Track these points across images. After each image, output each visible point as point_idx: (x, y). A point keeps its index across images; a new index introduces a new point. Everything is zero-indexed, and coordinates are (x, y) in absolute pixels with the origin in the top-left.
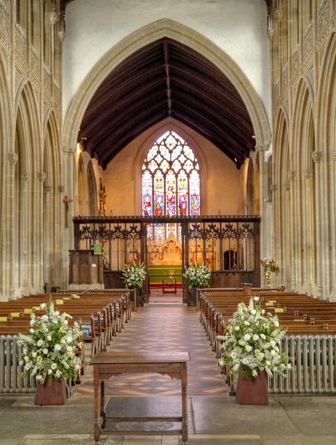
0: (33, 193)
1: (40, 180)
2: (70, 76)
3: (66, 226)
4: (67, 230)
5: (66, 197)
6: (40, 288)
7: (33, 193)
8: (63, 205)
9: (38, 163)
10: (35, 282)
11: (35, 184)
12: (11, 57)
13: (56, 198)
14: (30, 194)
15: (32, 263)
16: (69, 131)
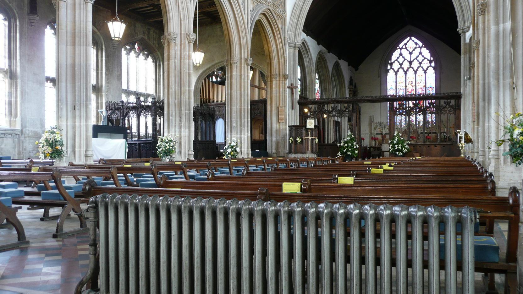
0: (241, 76)
1: (247, 64)
3: (293, 108)
5: (292, 84)
7: (241, 76)
11: (243, 68)
14: (238, 77)
15: (241, 134)
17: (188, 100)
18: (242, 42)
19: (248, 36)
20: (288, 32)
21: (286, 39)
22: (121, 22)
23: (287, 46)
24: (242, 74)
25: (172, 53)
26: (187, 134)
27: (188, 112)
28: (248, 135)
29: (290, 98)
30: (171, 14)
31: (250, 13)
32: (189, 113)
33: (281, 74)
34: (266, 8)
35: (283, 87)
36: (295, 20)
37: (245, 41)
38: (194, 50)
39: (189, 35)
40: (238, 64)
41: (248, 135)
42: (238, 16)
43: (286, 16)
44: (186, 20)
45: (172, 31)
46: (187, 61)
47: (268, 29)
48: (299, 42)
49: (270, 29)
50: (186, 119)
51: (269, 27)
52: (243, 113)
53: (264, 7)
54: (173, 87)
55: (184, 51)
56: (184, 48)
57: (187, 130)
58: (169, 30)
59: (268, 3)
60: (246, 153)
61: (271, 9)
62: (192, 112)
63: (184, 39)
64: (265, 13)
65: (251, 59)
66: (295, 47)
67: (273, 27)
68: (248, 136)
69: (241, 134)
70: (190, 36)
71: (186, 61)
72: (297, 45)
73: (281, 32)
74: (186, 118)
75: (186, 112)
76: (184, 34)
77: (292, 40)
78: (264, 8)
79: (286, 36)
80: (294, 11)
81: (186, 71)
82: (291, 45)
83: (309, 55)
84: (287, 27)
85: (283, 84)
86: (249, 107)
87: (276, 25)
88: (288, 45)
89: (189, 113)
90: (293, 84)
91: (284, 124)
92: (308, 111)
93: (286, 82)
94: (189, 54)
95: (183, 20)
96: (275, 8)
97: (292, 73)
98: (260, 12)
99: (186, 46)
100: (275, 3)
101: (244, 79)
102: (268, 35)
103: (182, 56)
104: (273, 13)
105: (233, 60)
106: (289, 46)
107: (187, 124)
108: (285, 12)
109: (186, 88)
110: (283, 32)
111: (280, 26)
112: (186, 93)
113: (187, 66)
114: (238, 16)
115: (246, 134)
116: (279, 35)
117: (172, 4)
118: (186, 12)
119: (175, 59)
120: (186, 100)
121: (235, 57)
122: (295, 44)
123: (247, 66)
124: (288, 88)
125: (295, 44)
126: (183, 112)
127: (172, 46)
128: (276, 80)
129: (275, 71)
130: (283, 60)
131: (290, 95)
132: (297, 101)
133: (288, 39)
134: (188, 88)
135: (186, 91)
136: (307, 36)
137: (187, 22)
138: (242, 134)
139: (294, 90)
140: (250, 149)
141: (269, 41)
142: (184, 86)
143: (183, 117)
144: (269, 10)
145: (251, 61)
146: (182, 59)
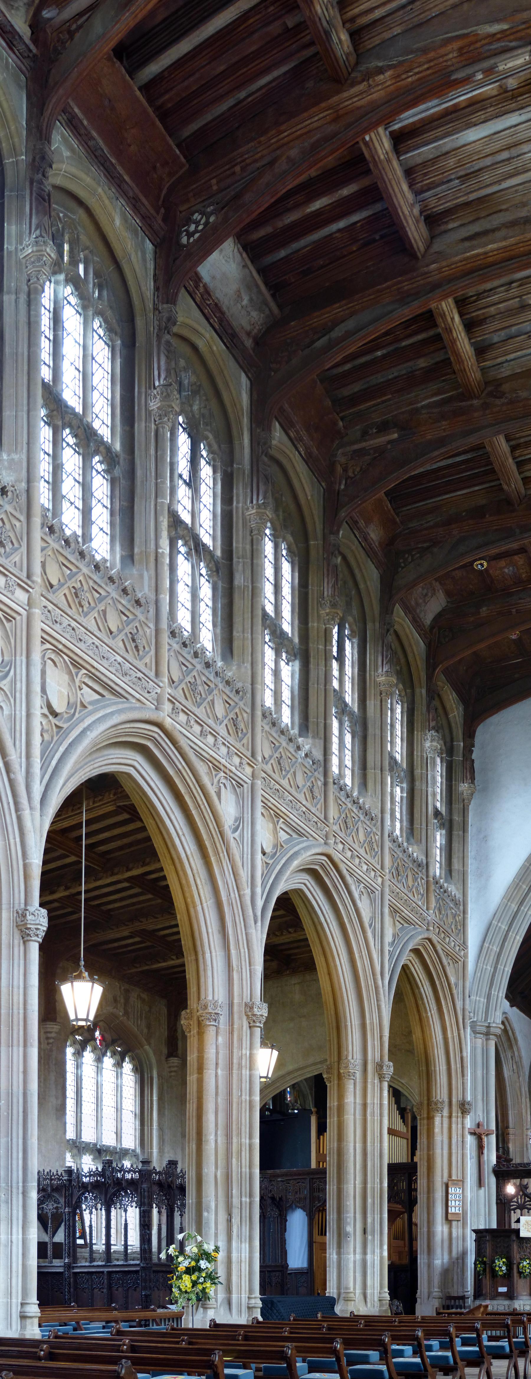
0: (365, 1105)
1: (381, 1078)
2: (484, 874)
3: (480, 1183)
4: (482, 1191)
5: (478, 1125)
6: (381, 1305)
7: (365, 1105)
8: (470, 1141)
9: (377, 1043)
10: (369, 1291)
11: (369, 1086)
12: (253, 786)
13: (454, 1126)
14: (359, 1108)
15: (364, 1253)
16: (485, 989)
17: (248, 1170)
18: (368, 1022)
19: (383, 1006)
20: (472, 997)
21: (467, 1013)
22: (92, 980)
23: (469, 1030)
24: (369, 1101)
25: (210, 1053)
26: (245, 1255)
27: (248, 1200)
28: (381, 1253)
29: (475, 1160)
30: (208, 955)
31: (387, 948)
32: (251, 1204)
33: (454, 1100)
34: (423, 936)
35: (460, 1132)
36: (489, 968)
37: (376, 1021)
38: (264, 1044)
39: (252, 1008)
40: (358, 1075)
41: (381, 1253)
42: (361, 957)
43: (466, 956)
44: (244, 970)
45: (210, 998)
46: (245, 1072)
47: (426, 989)
48: (496, 1019)
49: (430, 989)
50: (244, 1219)
51: (428, 984)
52: (369, 1200)
53: (419, 933)
54: (212, 1137)
55: (241, 1047)
56: (240, 1040)
57: (245, 1246)
58: (202, 997)
59: (428, 924)
60: (376, 1299)
61: (435, 939)
62: (257, 1199)
63: (240, 1018)
64: (420, 947)
65: (391, 1064)
66: (487, 1034)
67: (437, 983)
68: (382, 1258)
69: (364, 1253)
70: (255, 1010)
71: (244, 1072)
72: (492, 1030)
73: (455, 991)
74: (244, 1215)
75: (244, 1199)
76: (239, 1005)
77: (480, 1016)
78: (420, 937)
79: (467, 1007)
80: (486, 945)
81: (243, 1097)
82: (478, 1029)
83: (516, 1053)
84: (468, 985)
85: (460, 1126)
86: (386, 1184)
87: (443, 979)
88: (471, 1028)
89: (251, 1204)
90: (483, 1126)
91: (460, 1223)
92: (516, 1195)
93: (466, 1122)
94: (251, 1054)
95: (237, 971)
96: (443, 935)
97: (480, 1097)
98: (410, 946)
99: (244, 1034)
100: (442, 923)
101: (373, 1114)
102: (423, 1004)
103: (235, 1061)
104: (439, 948)
105: (346, 1067)
106: (474, 1032)
107: (246, 1230)
108: (464, 945)
109: (243, 1140)
110: (461, 996)
111: (453, 980)
112: (243, 1153)
113: (246, 1086)
114: (361, 957)
115: (377, 1251)
116: (450, 1004)
117: (210, 931)
118: (244, 950)
119: (217, 1068)
120: (243, 1170)
121: (350, 1058)
122: (489, 1027)
123: (381, 1082)
124: (471, 1134)
125: (489, 1027)
126: (236, 1201)
127: (210, 1033)
128: (442, 1116)
129: (441, 1093)
130: (459, 1065)
131: (475, 1154)
132: (491, 1170)
133: (472, 1015)
134: (247, 1141)
135: (243, 1149)
136: (512, 1006)
137: (246, 974)
138: (369, 1251)
139: (485, 1139)
140: (386, 1290)
141: (427, 1017)
142: (239, 1134)
143: (236, 1212)
144: (430, 940)
145: (389, 1069)
146: (235, 1066)
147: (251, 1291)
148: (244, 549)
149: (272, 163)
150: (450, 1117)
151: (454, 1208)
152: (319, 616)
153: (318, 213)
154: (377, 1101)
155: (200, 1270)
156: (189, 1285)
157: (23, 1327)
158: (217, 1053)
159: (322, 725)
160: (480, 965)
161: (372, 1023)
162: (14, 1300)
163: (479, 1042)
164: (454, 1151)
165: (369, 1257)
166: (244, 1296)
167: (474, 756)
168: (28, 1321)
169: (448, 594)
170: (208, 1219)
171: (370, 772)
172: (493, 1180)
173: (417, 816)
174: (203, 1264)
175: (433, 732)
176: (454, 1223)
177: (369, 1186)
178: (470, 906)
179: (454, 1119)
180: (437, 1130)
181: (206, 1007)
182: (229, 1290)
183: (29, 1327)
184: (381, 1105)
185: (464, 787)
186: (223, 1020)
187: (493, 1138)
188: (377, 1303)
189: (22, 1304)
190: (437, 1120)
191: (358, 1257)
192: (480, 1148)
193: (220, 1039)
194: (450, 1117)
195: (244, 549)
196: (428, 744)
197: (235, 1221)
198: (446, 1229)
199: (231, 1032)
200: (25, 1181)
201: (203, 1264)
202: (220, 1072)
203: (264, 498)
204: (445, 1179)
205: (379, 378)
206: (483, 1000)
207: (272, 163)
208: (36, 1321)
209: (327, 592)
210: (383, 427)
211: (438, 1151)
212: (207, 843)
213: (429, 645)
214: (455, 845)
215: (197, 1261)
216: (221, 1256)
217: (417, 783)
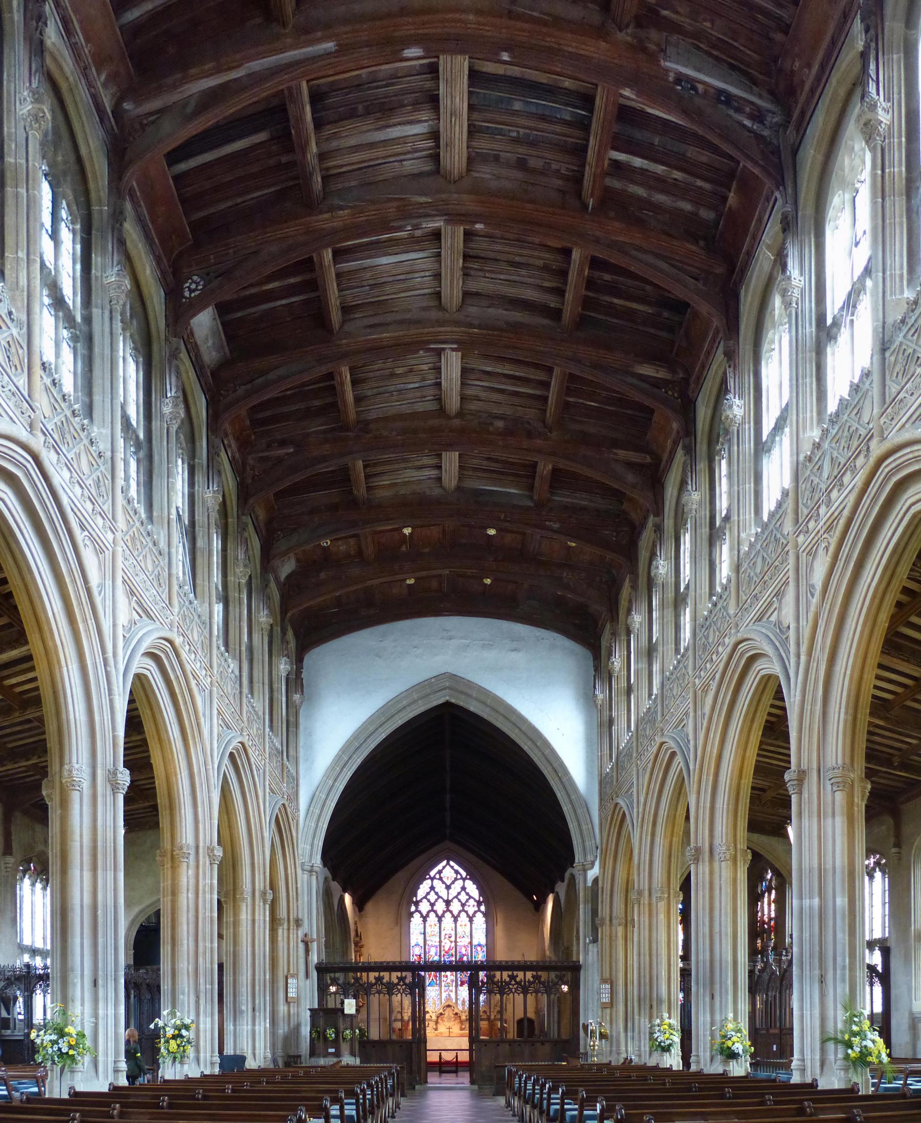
0: (253, 921)
3: (307, 976)
4: (308, 981)
5: (306, 935)
7: (253, 921)
8: (301, 946)
11: (257, 907)
14: (249, 922)
15: (254, 1024)
18: (256, 862)
26: (209, 1026)
37: (261, 862)
42: (254, 816)
43: (298, 816)
52: (257, 988)
55: (204, 879)
57: (209, 1020)
63: (204, 857)
66: (311, 871)
68: (265, 1028)
69: (254, 1024)
76: (204, 847)
97: (306, 915)
105: (242, 894)
106: (303, 870)
108: (298, 810)
114: (254, 816)
115: (262, 1023)
126: (202, 987)
138: (257, 1023)
142: (204, 940)
143: (202, 996)
147: (213, 1051)
148: (203, 521)
149: (256, 253)
150: (289, 929)
151: (292, 993)
152: (235, 573)
153: (271, 291)
154: (262, 918)
155: (182, 1036)
156: (176, 1047)
157: (116, 1078)
158: (188, 882)
159: (238, 651)
160: (307, 822)
161: (259, 863)
162: (109, 1059)
163: (306, 876)
164: (291, 953)
165: (257, 1027)
166: (208, 1055)
167: (303, 676)
168: (120, 1074)
169: (298, 560)
170: (183, 1000)
171: (256, 686)
172: (315, 974)
173: (275, 717)
174: (184, 1032)
175: (285, 658)
176: (292, 1004)
177: (257, 978)
178: (301, 781)
179: (291, 931)
180: (280, 939)
181: (181, 848)
182: (198, 1051)
183: (120, 1078)
184: (265, 921)
185: (296, 697)
186: (192, 858)
187: (315, 944)
188: (262, 1060)
189: (115, 1062)
190: (280, 931)
191: (250, 1027)
192: (307, 951)
193: (190, 872)
194: (289, 929)
195: (203, 521)
196: (282, 667)
197: (202, 1002)
198: (286, 1008)
199: (197, 867)
200: (116, 971)
201: (184, 1032)
202: (190, 895)
203: (218, 486)
204: (286, 973)
205: (286, 409)
206: (309, 847)
207: (256, 253)
208: (125, 1074)
209: (241, 556)
210: (283, 443)
211: (281, 953)
212: (189, 731)
213: (282, 597)
214: (291, 738)
215: (180, 1030)
216: (193, 1026)
217: (275, 694)
